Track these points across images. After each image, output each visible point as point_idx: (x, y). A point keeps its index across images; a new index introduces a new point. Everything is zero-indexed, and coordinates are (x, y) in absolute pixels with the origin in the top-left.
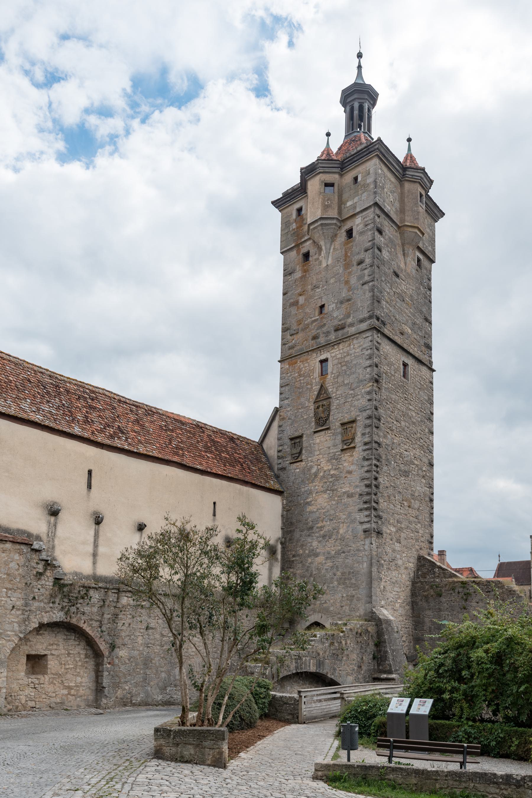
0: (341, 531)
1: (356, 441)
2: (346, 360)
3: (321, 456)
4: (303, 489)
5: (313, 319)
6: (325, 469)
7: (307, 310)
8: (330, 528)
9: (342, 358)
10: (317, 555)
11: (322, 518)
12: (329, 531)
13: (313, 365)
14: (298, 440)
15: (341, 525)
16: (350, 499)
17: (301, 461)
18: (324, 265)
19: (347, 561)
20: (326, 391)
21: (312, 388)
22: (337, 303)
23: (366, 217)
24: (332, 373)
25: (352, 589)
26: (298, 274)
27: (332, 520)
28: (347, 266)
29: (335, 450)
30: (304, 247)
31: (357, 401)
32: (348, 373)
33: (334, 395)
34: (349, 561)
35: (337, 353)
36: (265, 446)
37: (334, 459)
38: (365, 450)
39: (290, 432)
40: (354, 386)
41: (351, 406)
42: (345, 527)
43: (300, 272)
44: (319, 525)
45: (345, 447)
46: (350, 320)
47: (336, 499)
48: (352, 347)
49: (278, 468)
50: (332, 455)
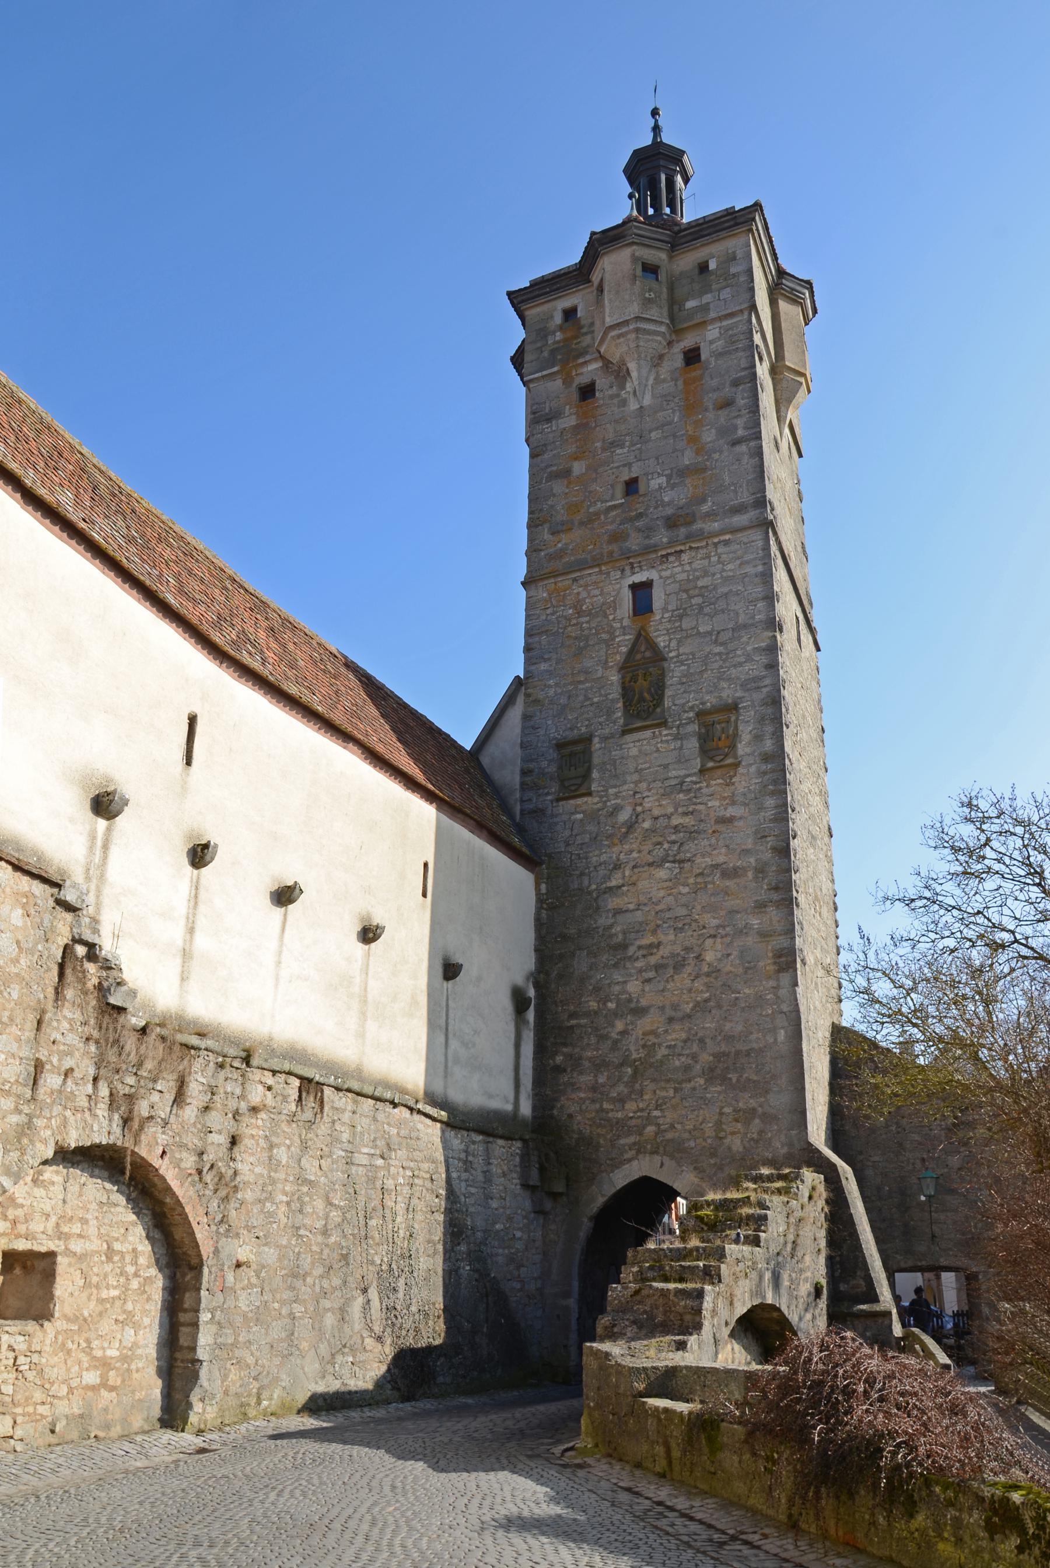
0: (709, 957)
1: (740, 752)
2: (700, 583)
3: (644, 785)
4: (595, 859)
5: (610, 504)
6: (656, 812)
7: (595, 487)
8: (678, 949)
9: (688, 580)
10: (640, 1012)
11: (652, 926)
12: (673, 955)
13: (613, 593)
14: (579, 748)
15: (709, 942)
16: (728, 883)
17: (589, 794)
18: (633, 405)
19: (728, 1026)
20: (652, 646)
21: (613, 639)
22: (669, 477)
23: (731, 329)
24: (665, 609)
25: (747, 1095)
26: (569, 421)
27: (682, 930)
29: (682, 773)
30: (582, 374)
31: (735, 666)
32: (707, 610)
33: (671, 655)
34: (734, 1027)
35: (676, 570)
36: (485, 760)
37: (681, 791)
38: (765, 773)
39: (553, 729)
40: (723, 637)
41: (720, 679)
42: (719, 947)
43: (574, 417)
44: (645, 942)
45: (711, 764)
46: (705, 508)
47: (691, 881)
48: (714, 559)
49: (522, 810)
50: (673, 782)
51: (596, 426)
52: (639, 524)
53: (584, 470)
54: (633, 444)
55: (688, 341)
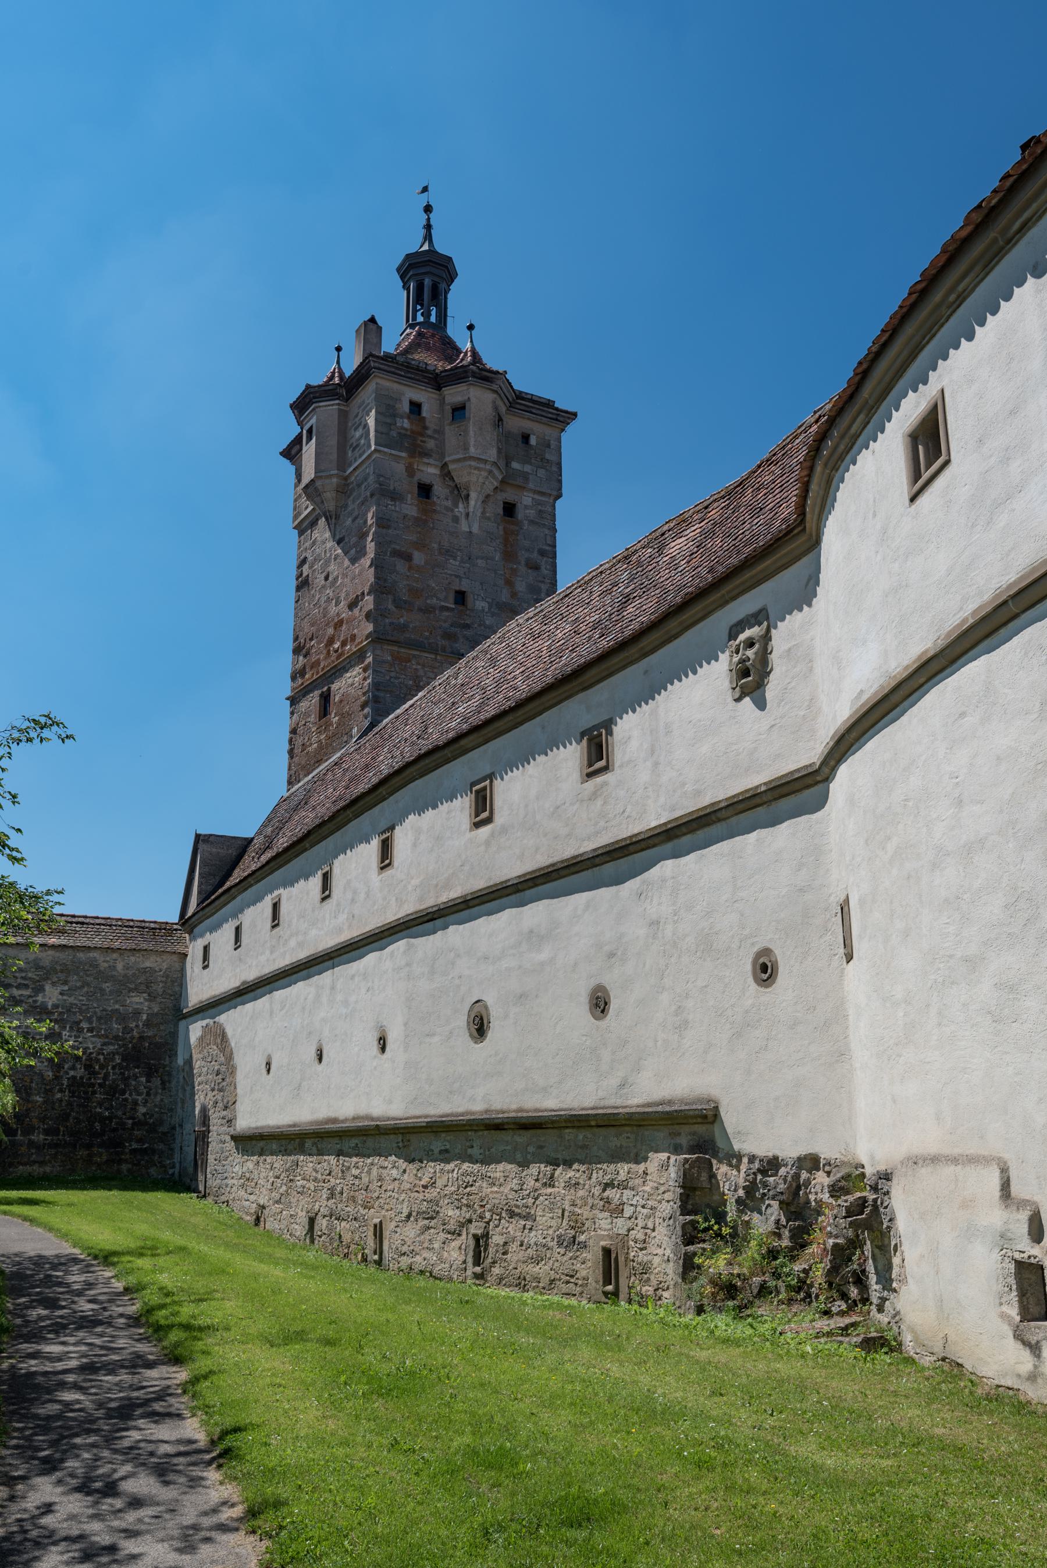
5: (443, 604)
22: (490, 606)
28: (509, 555)
51: (433, 528)
52: (468, 633)
53: (423, 563)
54: (462, 561)
55: (510, 495)
